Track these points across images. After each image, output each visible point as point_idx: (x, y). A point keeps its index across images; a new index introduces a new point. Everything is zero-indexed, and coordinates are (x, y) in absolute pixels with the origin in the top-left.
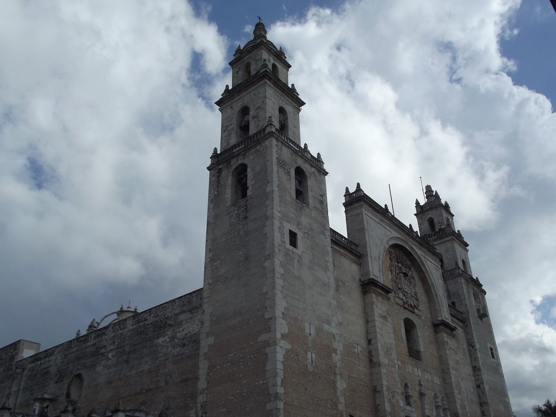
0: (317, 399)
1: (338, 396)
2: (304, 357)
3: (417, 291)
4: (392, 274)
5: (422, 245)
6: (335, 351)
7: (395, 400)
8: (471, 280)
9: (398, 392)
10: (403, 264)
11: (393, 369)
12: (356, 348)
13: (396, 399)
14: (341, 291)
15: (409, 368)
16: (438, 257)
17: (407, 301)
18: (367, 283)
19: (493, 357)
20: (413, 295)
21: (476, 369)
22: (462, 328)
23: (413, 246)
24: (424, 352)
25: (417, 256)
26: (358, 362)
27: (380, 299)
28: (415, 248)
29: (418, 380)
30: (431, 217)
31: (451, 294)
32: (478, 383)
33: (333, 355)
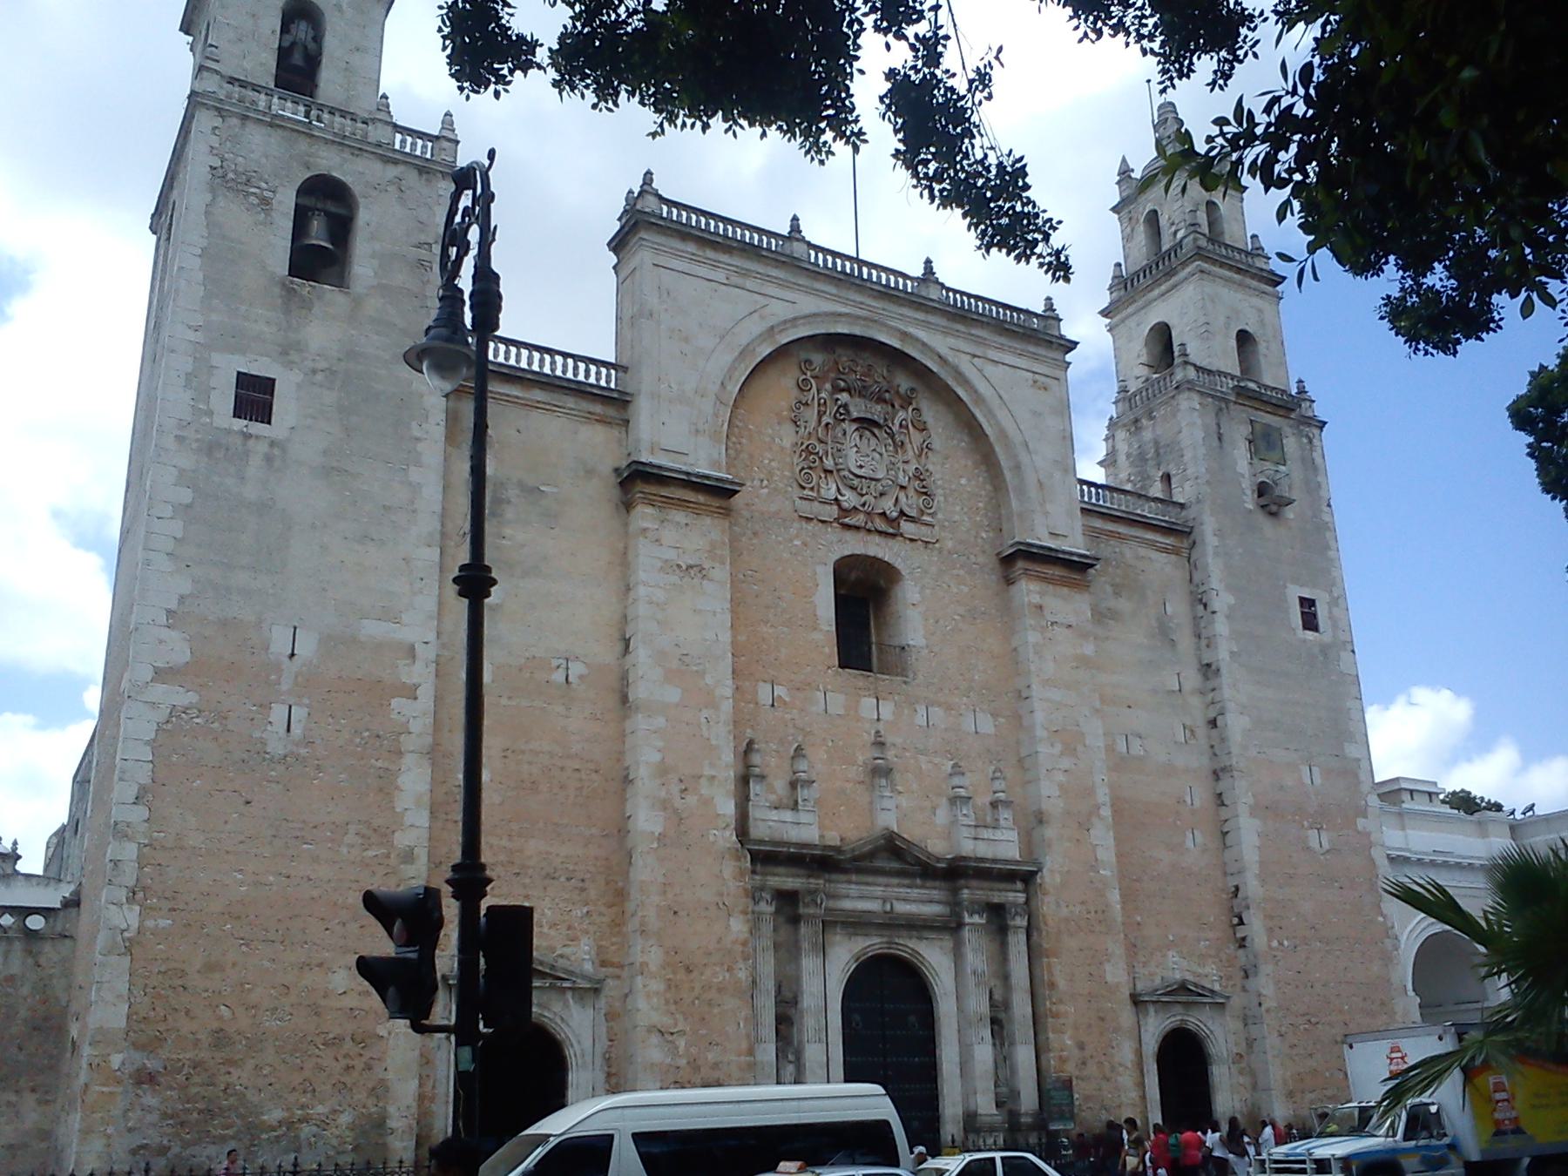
0: (300, 826)
1: (398, 810)
2: (252, 719)
3: (931, 467)
4: (797, 432)
6: (411, 693)
7: (692, 799)
8: (1238, 395)
9: (713, 777)
10: (862, 392)
11: (705, 713)
12: (562, 672)
13: (701, 795)
15: (837, 703)
17: (864, 505)
18: (626, 478)
19: (1310, 622)
20: (903, 481)
21: (1208, 670)
22: (1176, 551)
23: (911, 330)
24: (927, 646)
25: (936, 357)
26: (560, 709)
27: (679, 516)
28: (922, 334)
29: (873, 732)
30: (1152, 208)
31: (1162, 451)
32: (1212, 715)
33: (395, 702)
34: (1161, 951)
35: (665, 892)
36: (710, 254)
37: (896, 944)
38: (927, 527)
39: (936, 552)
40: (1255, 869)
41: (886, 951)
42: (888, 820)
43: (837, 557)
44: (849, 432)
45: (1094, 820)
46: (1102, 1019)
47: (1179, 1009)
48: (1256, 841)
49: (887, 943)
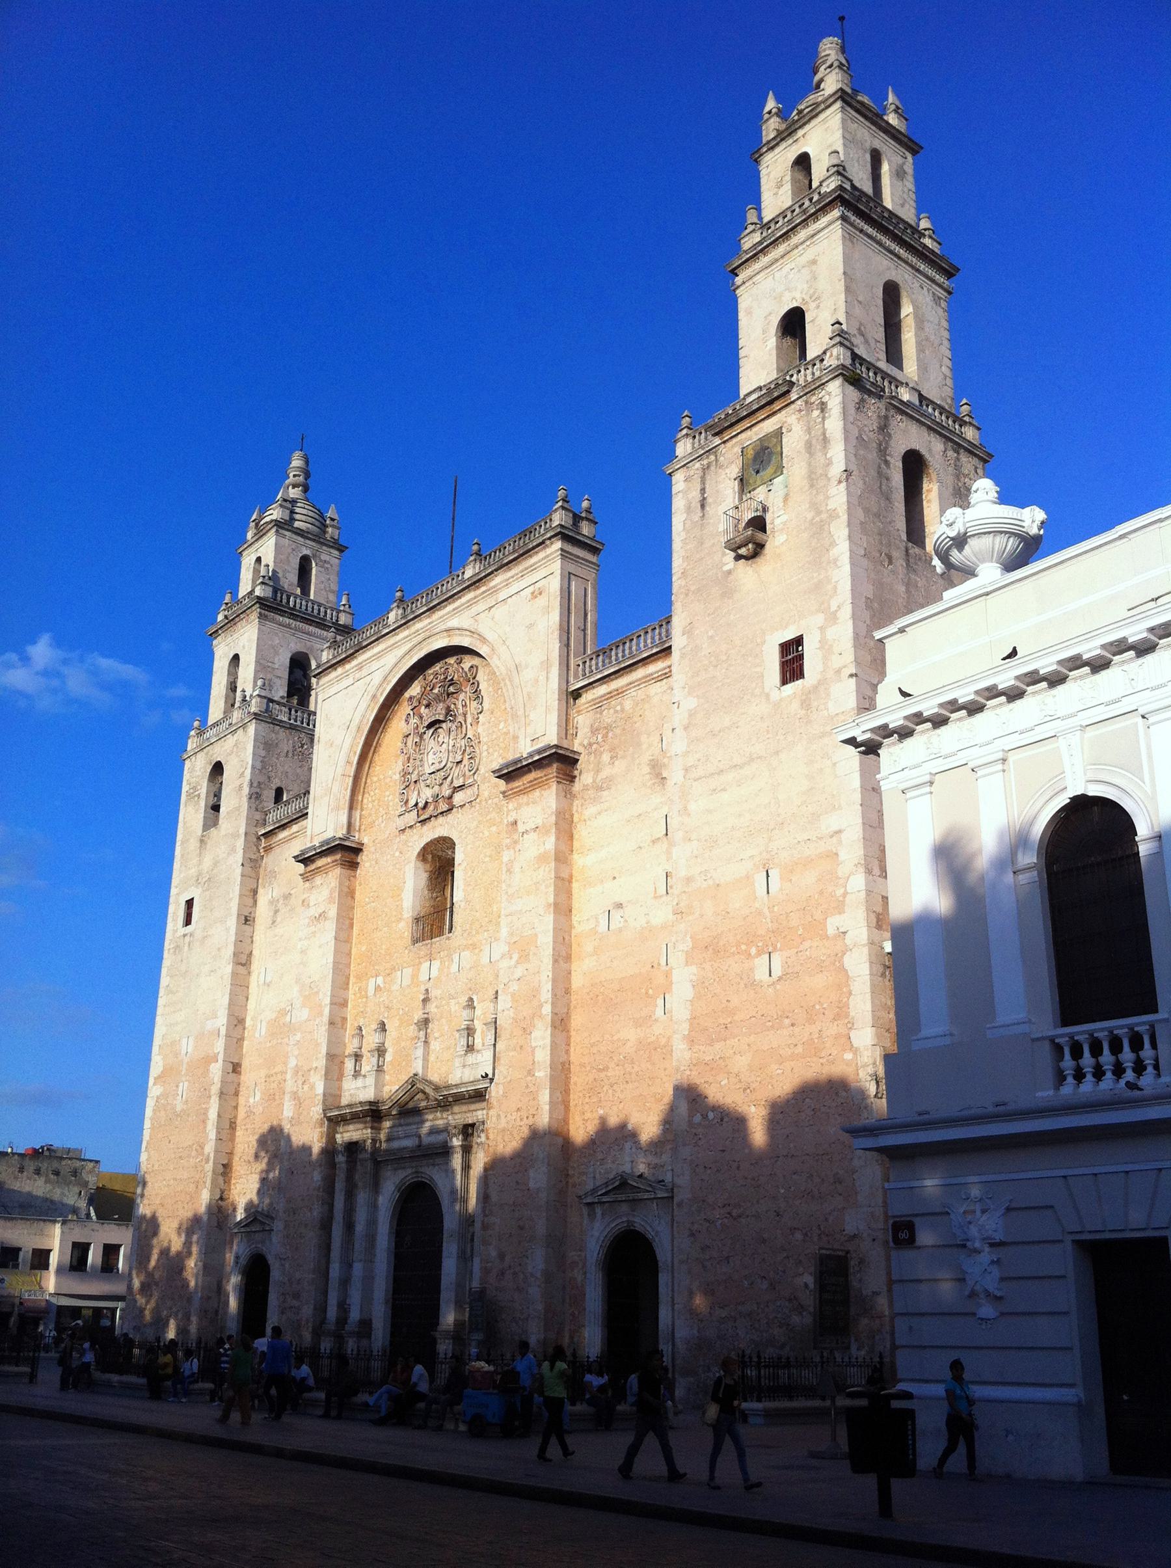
3: (480, 730)
5: (481, 579)
7: (306, 1087)
9: (316, 1067)
14: (279, 919)
16: (548, 542)
20: (459, 759)
25: (468, 633)
28: (454, 623)
29: (424, 992)
34: (618, 1146)
35: (290, 1158)
36: (348, 666)
37: (422, 1172)
38: (470, 789)
39: (478, 805)
40: (685, 1028)
41: (416, 1180)
42: (418, 1067)
43: (416, 853)
44: (427, 741)
45: (536, 1021)
46: (521, 1228)
47: (625, 1207)
48: (689, 993)
49: (416, 1172)
